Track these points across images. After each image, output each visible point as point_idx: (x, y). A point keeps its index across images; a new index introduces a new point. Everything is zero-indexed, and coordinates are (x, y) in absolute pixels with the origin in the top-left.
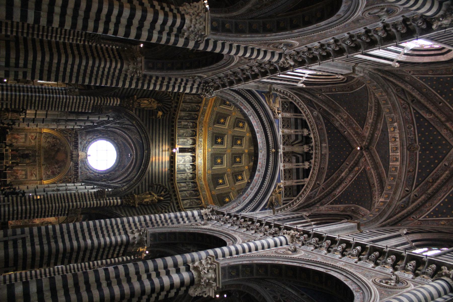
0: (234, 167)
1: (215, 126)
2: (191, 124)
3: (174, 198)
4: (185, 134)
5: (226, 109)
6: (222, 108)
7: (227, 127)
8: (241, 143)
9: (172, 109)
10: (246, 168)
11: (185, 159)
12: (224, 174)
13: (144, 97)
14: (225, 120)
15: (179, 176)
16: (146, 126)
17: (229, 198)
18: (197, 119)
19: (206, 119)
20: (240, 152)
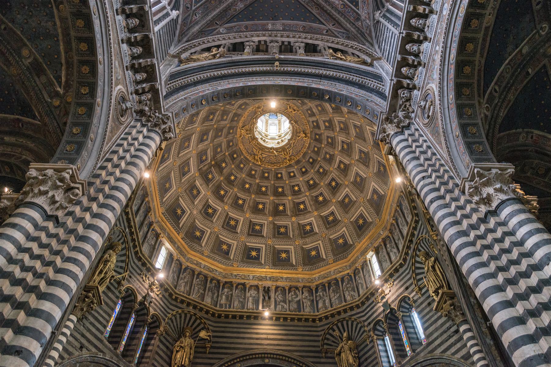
0: (293, 236)
1: (232, 258)
2: (226, 290)
3: (343, 315)
4: (241, 300)
5: (208, 239)
6: (206, 243)
7: (235, 243)
8: (259, 225)
9: (199, 314)
10: (294, 219)
11: (281, 301)
12: (302, 249)
13: (170, 358)
14: (225, 243)
15: (308, 310)
16: (222, 359)
17: (338, 238)
18: (218, 281)
19: (221, 268)
20: (271, 226)
